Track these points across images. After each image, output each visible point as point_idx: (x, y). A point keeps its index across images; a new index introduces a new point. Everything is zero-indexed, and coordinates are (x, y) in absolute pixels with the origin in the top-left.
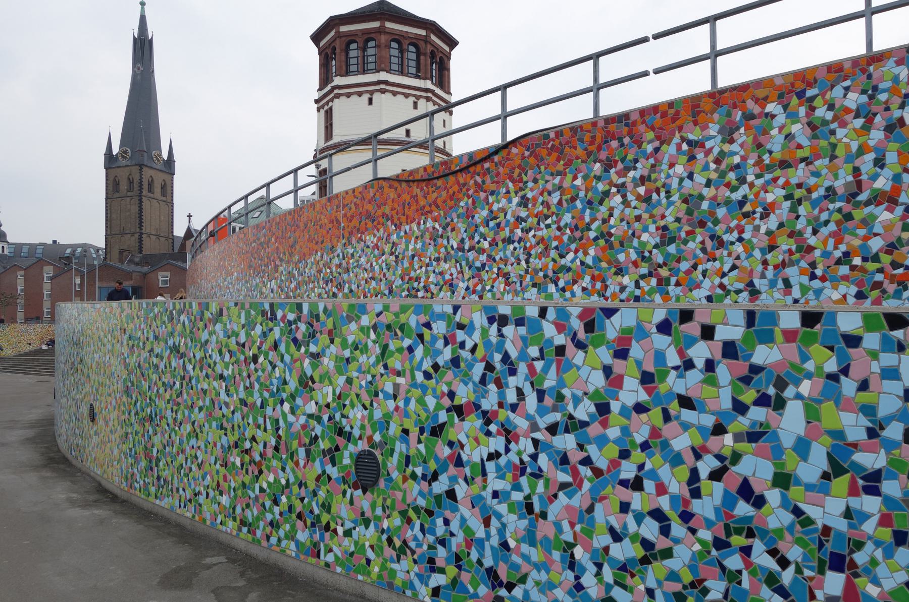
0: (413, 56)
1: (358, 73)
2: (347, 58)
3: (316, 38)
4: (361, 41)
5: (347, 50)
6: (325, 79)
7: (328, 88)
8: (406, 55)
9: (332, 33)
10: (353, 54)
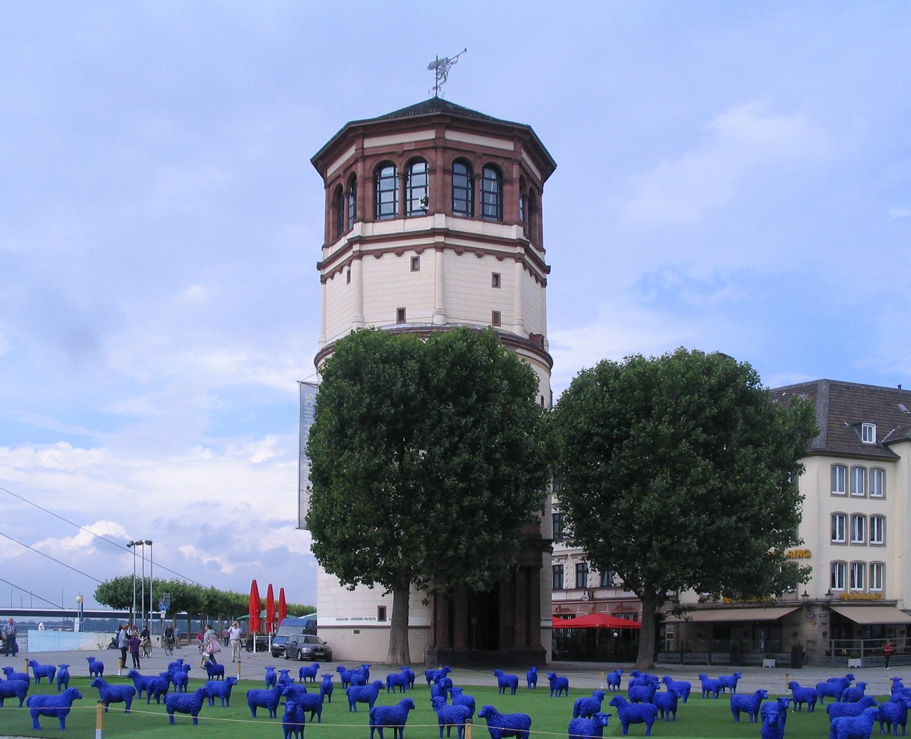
0: (492, 186)
1: (395, 216)
2: (376, 193)
3: (321, 161)
4: (401, 162)
5: (376, 179)
6: (337, 226)
7: (343, 242)
8: (478, 184)
9: (351, 152)
10: (384, 185)
